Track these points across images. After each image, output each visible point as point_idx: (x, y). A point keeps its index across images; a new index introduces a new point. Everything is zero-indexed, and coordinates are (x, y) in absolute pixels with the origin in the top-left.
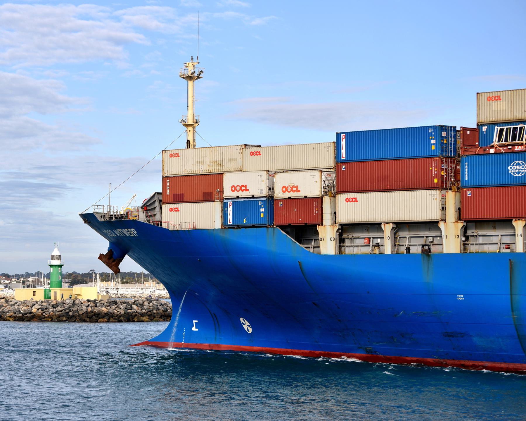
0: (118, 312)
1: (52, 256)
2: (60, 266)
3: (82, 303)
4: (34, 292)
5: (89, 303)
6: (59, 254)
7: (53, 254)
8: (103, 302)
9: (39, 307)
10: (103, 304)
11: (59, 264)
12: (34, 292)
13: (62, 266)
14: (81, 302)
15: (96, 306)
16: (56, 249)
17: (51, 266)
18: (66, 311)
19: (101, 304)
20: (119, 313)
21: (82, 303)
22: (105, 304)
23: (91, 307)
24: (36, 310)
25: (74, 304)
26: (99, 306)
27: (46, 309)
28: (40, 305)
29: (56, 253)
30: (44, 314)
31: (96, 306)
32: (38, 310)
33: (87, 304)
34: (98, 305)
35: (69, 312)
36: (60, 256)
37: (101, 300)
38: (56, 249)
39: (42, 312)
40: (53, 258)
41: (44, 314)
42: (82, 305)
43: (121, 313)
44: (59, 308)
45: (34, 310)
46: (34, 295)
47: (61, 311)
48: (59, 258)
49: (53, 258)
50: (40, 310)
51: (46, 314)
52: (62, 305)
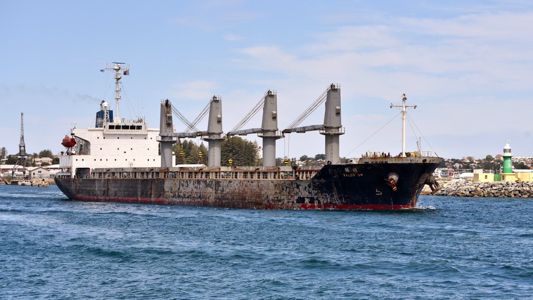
1: (504, 149)
2: (510, 157)
4: (486, 176)
6: (510, 148)
7: (505, 148)
8: (528, 183)
9: (482, 187)
10: (528, 185)
11: (510, 156)
12: (486, 176)
15: (523, 186)
16: (507, 145)
17: (506, 158)
21: (513, 184)
23: (519, 187)
27: (486, 188)
29: (507, 147)
30: (484, 192)
31: (523, 186)
32: (481, 188)
33: (516, 185)
34: (524, 185)
35: (501, 190)
36: (510, 149)
37: (528, 182)
38: (507, 145)
41: (484, 192)
44: (494, 188)
45: (479, 189)
46: (486, 178)
47: (496, 190)
48: (510, 151)
49: (505, 151)
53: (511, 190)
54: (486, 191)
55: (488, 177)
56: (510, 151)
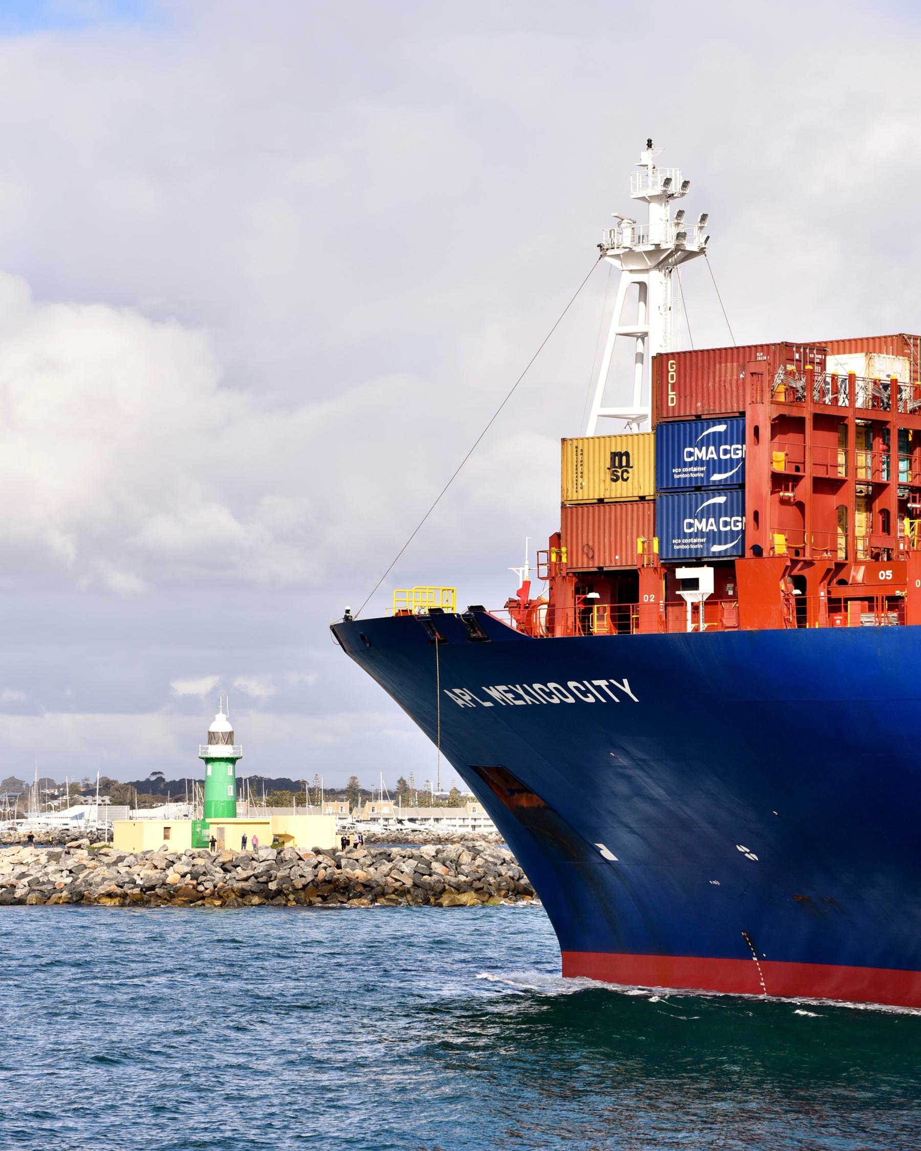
0: (397, 880)
1: (209, 732)
2: (232, 761)
3: (300, 859)
4: (167, 829)
5: (320, 858)
7: (213, 729)
9: (187, 869)
10: (357, 860)
12: (167, 829)
13: (238, 761)
14: (298, 854)
15: (339, 867)
17: (208, 760)
18: (261, 880)
19: (351, 861)
20: (399, 884)
21: (300, 859)
22: (362, 860)
23: (325, 868)
24: (178, 876)
25: (280, 861)
26: (346, 866)
27: (204, 874)
28: (188, 865)
30: (201, 888)
31: (339, 867)
32: (183, 876)
33: (314, 861)
35: (266, 883)
36: (231, 734)
39: (195, 882)
40: (212, 738)
42: (300, 862)
43: (404, 884)
44: (241, 873)
45: (172, 877)
46: (166, 837)
47: (246, 879)
48: (229, 738)
49: (212, 738)
50: (189, 876)
51: (206, 889)
52: (247, 865)
53: (304, 881)
54: (209, 885)
55: (172, 832)
56: (229, 738)
